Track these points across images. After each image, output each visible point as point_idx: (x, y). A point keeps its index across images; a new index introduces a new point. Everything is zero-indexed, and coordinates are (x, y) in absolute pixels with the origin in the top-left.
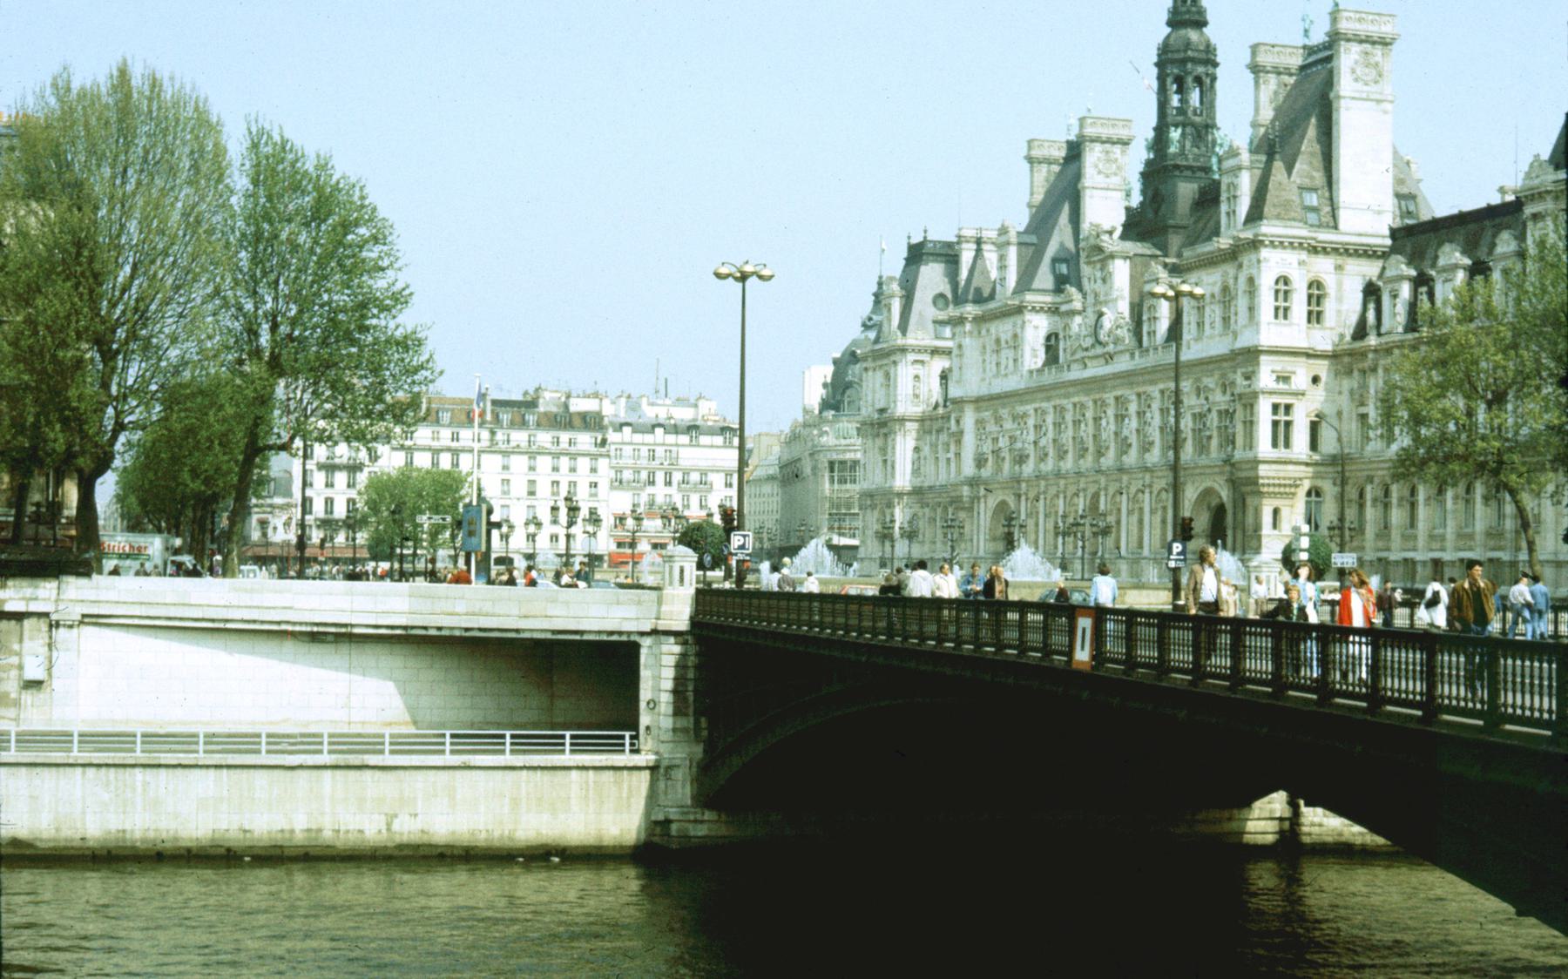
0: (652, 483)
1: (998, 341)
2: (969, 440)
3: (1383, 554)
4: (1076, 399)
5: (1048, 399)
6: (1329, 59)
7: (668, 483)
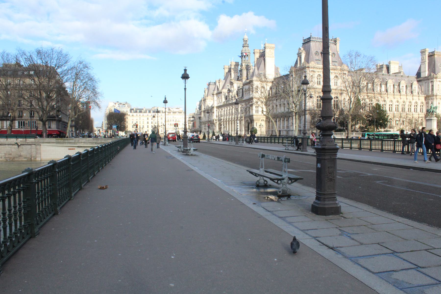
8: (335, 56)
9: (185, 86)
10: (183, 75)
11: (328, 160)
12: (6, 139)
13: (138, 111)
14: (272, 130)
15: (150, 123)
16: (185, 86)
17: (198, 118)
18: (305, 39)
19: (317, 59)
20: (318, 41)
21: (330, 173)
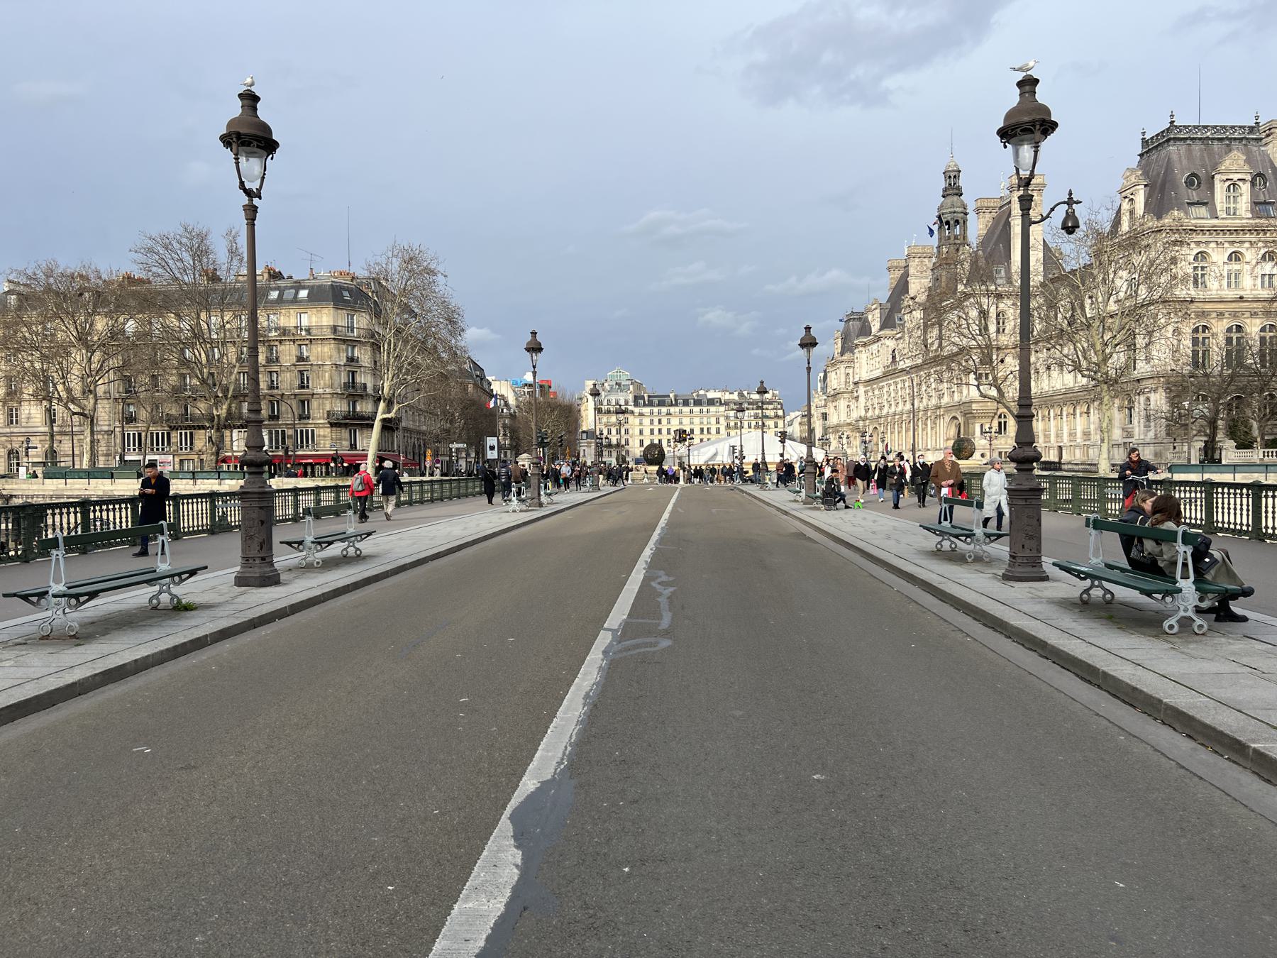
2: (862, 399)
3: (1047, 445)
5: (891, 379)
6: (1010, 202)
8: (1265, 183)
12: (191, 482)
13: (656, 401)
15: (647, 431)
17: (820, 415)
18: (1148, 137)
19: (1196, 199)
20: (1200, 139)
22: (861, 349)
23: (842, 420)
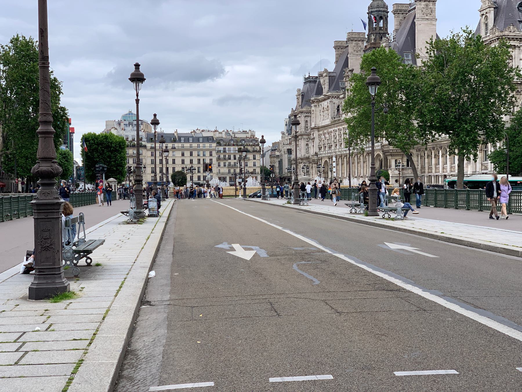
0: (230, 159)
1: (323, 108)
2: (317, 141)
4: (343, 126)
6: (415, 8)
7: (235, 159)
9: (137, 95)
10: (132, 75)
11: (42, 220)
14: (436, 174)
16: (137, 95)
17: (286, 151)
21: (45, 239)
22: (315, 104)
23: (303, 154)
